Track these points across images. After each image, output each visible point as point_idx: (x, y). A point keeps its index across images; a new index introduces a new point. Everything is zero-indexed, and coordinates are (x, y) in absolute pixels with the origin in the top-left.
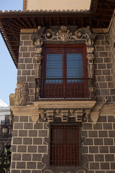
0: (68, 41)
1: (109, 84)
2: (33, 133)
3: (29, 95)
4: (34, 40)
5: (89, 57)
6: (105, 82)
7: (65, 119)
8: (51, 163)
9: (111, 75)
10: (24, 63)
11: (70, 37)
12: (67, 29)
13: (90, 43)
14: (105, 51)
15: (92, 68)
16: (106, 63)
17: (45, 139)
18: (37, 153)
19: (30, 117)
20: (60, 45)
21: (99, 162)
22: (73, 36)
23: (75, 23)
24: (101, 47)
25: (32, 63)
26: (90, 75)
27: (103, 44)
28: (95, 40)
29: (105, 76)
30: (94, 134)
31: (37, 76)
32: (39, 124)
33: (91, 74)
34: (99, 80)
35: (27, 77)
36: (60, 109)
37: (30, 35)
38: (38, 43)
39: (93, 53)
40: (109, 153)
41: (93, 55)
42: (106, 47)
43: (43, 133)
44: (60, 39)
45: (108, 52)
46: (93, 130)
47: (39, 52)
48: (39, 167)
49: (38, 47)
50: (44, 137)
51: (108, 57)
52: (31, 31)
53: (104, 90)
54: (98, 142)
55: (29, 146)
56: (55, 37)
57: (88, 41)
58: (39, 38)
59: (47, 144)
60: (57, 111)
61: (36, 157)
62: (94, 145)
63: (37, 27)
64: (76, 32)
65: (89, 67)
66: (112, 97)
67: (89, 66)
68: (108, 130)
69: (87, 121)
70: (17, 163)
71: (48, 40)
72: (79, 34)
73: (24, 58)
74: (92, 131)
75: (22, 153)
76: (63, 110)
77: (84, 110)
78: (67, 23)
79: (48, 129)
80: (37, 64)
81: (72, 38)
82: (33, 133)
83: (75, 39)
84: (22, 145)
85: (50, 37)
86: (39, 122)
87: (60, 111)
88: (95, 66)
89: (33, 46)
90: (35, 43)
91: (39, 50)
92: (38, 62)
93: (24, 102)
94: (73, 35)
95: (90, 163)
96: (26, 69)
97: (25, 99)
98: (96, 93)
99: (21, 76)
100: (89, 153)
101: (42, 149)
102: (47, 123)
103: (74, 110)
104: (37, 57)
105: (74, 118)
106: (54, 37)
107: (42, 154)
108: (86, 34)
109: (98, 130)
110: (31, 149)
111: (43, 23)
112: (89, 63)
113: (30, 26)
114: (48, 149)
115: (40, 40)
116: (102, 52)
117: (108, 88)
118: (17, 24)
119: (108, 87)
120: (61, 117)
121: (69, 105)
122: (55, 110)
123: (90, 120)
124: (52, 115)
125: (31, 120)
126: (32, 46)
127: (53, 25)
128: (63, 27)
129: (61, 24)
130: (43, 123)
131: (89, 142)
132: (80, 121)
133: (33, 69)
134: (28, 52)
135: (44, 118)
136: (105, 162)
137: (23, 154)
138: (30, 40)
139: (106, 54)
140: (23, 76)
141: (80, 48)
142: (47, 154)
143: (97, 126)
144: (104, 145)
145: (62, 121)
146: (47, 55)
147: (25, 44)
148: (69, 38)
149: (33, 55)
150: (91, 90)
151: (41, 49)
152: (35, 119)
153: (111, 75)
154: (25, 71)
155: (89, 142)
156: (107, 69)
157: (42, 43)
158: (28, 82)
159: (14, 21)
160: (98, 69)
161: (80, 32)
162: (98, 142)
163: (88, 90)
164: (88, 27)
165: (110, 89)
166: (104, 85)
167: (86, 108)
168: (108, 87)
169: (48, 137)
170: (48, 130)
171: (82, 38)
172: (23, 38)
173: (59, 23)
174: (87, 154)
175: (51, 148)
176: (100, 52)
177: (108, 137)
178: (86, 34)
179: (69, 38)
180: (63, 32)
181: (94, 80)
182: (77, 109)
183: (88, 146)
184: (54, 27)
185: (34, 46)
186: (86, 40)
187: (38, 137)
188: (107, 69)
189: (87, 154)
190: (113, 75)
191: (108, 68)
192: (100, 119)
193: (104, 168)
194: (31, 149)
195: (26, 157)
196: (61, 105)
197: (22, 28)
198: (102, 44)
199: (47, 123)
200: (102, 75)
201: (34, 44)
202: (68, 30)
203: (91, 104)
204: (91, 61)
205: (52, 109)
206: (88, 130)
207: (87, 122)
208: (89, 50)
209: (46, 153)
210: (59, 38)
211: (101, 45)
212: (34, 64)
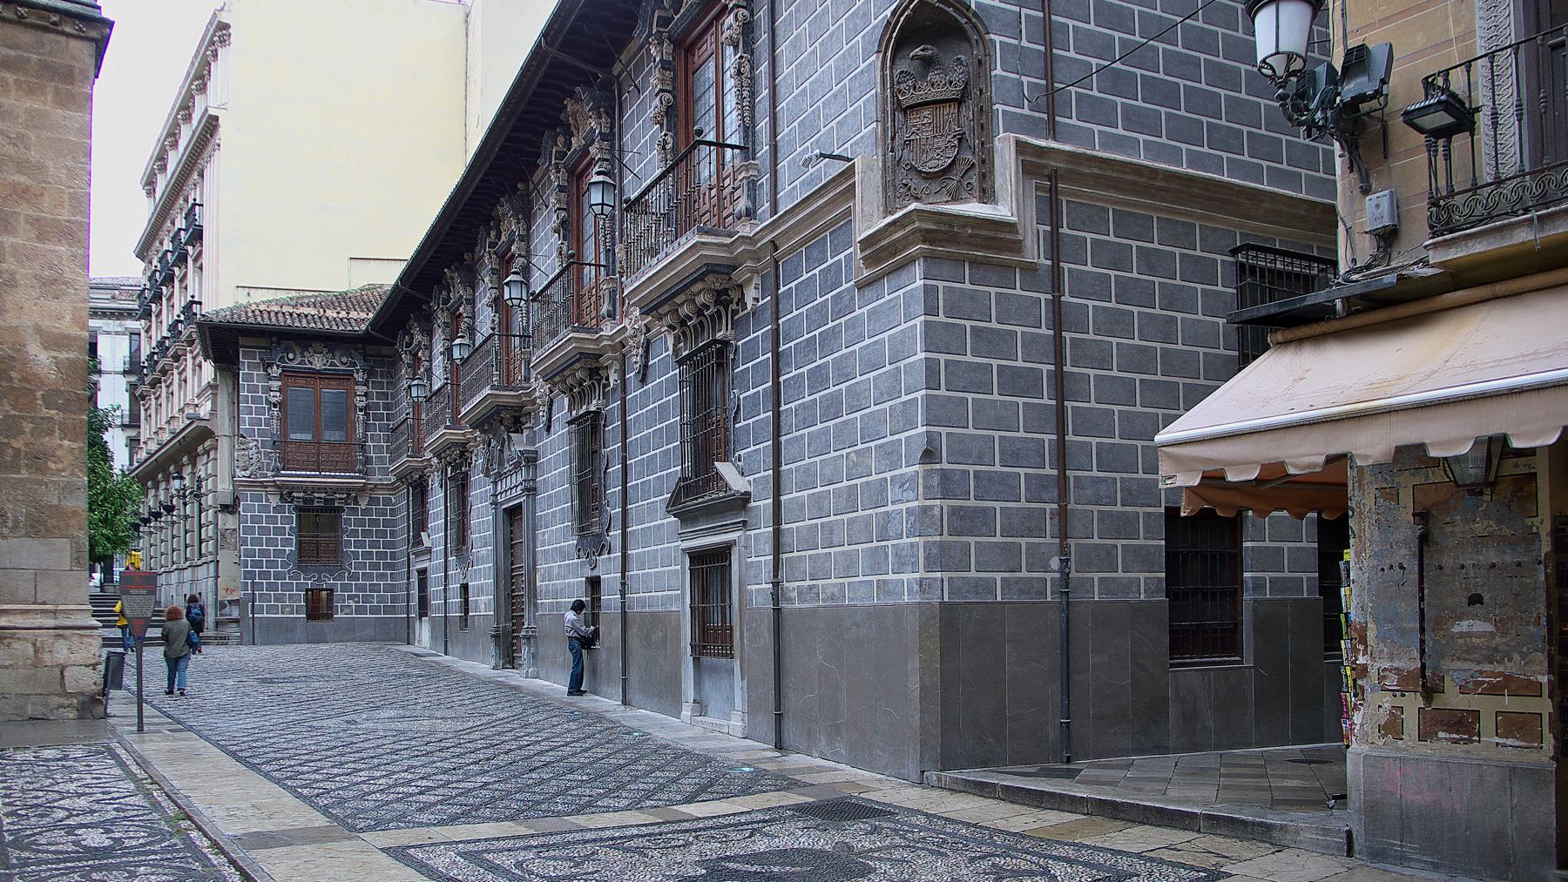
2: (272, 520)
4: (267, 366)
13: (359, 377)
38: (275, 371)
39: (366, 395)
43: (288, 520)
91: (276, 384)
101: (286, 542)
143: (366, 512)
162: (366, 533)
175: (300, 544)
194: (270, 542)
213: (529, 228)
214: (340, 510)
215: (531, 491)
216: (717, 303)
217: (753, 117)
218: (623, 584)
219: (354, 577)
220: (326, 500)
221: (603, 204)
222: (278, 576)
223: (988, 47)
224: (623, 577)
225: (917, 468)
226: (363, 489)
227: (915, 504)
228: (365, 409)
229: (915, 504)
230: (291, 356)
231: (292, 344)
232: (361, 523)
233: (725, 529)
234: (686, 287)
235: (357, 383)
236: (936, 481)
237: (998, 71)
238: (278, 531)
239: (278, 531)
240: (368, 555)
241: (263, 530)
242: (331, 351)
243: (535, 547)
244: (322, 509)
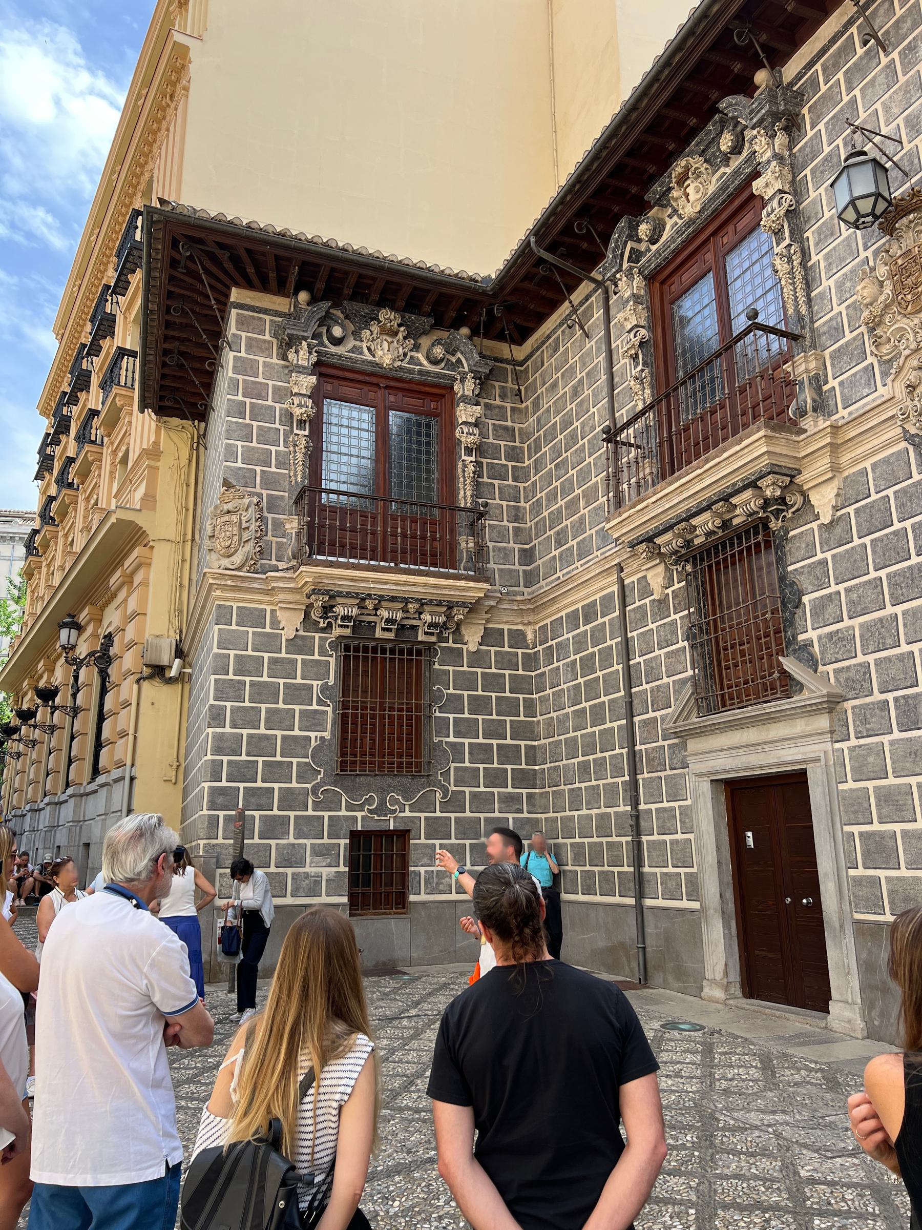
0: (400, 367)
1: (517, 531)
2: (282, 667)
3: (269, 537)
4: (288, 343)
5: (466, 437)
6: (505, 523)
7: (390, 630)
8: (343, 765)
9: (522, 504)
10: (247, 421)
11: (405, 355)
12: (400, 325)
13: (468, 387)
14: (509, 423)
15: (472, 475)
16: (510, 464)
17: (324, 689)
18: (297, 732)
19: (273, 611)
20: (372, 374)
21: (481, 766)
22: (415, 354)
23: (427, 309)
24: (499, 407)
25: (277, 425)
26: (465, 497)
28: (484, 381)
29: (504, 503)
30: (468, 682)
31: (299, 476)
32: (303, 637)
33: (469, 493)
35: (258, 472)
36: (381, 598)
37: (268, 318)
38: (303, 356)
40: (509, 741)
41: (476, 431)
42: (513, 409)
43: (316, 669)
44: (374, 356)
45: (517, 426)
46: (465, 668)
47: (304, 392)
48: (301, 778)
49: (300, 369)
50: (320, 683)
51: (517, 444)
52: (281, 303)
53: (500, 549)
54: (479, 705)
55: (268, 711)
56: (358, 343)
57: (463, 381)
58: (305, 338)
59: (329, 706)
60: (370, 604)
61: (293, 745)
62: (466, 715)
63: (296, 293)
64: (425, 342)
65: (464, 471)
66: (521, 574)
67: (465, 466)
68: (507, 672)
69: (451, 641)
70: (230, 763)
71: (333, 349)
72: (438, 351)
73: (248, 401)
74: (464, 672)
75: (245, 732)
76: (387, 600)
78: (401, 304)
79: (331, 656)
80: (296, 431)
82: (282, 667)
83: (421, 364)
84: (247, 704)
85: (338, 342)
86: (301, 633)
87: (380, 601)
89: (278, 362)
90: (291, 356)
92: (301, 423)
93: (252, 559)
94: (416, 347)
95: (456, 768)
96: (254, 444)
97: (258, 549)
98: (481, 551)
99: (239, 465)
100: (452, 739)
101: (312, 720)
102: (327, 638)
103: (422, 603)
104: (298, 406)
105: (414, 628)
106: (351, 343)
107: (312, 735)
108: (459, 355)
109: (479, 670)
110: (277, 719)
111: (320, 285)
112: (464, 457)
113: (255, 279)
114: (334, 720)
115: (309, 345)
116: (500, 426)
117: (511, 545)
118: (228, 265)
119: (511, 541)
120: (376, 623)
121: (410, 589)
122: (363, 600)
123: (459, 639)
124: (355, 611)
125: (275, 623)
126: (274, 360)
127: (354, 297)
128: (385, 315)
129: (382, 303)
130: (317, 635)
131: (455, 704)
132: (433, 639)
133: (282, 448)
134: (260, 379)
135: (321, 621)
136: (496, 765)
137: (250, 736)
138: (267, 337)
139: (510, 432)
140: (245, 466)
142: (327, 735)
143: (478, 659)
144: (494, 717)
145: (379, 633)
146: (325, 402)
147: (249, 348)
148: (402, 358)
149: (281, 394)
150: (466, 544)
151: (313, 379)
152: (290, 624)
153: (522, 504)
154: (253, 448)
155: (455, 704)
156: (510, 482)
157: (314, 358)
158: (265, 492)
159: (224, 256)
160: (485, 479)
161: (439, 343)
162: (479, 705)
164: (465, 331)
165: (516, 546)
167: (458, 602)
168: (511, 541)
169: (331, 682)
170: (332, 661)
171: (443, 365)
172: (243, 324)
173: (375, 297)
174: (447, 739)
175: (344, 721)
176: (494, 425)
177: (508, 694)
178: (459, 355)
179: (402, 358)
180: (384, 331)
181: (479, 514)
182: (430, 603)
183: (451, 716)
184: (356, 306)
185: (283, 362)
186: (458, 377)
187: (299, 680)
188: (510, 482)
189: (447, 739)
190: (527, 506)
191: (515, 480)
192: (490, 637)
193: (493, 783)
194: (277, 719)
195: (259, 745)
196: (388, 587)
197: (237, 285)
198: (500, 396)
199: (327, 638)
200: (498, 501)
201: (285, 358)
202: (402, 329)
203: (474, 590)
204: (469, 451)
205: (357, 594)
206: (451, 669)
207: (451, 644)
208: (465, 413)
209: (324, 734)
210: (369, 349)
211: (498, 402)
212: (282, 428)
219: (454, 802)
222: (290, 800)
226: (473, 608)
228: (479, 450)
232: (468, 682)
235: (465, 399)
238: (298, 694)
239: (298, 694)
240: (482, 753)
241: (263, 692)
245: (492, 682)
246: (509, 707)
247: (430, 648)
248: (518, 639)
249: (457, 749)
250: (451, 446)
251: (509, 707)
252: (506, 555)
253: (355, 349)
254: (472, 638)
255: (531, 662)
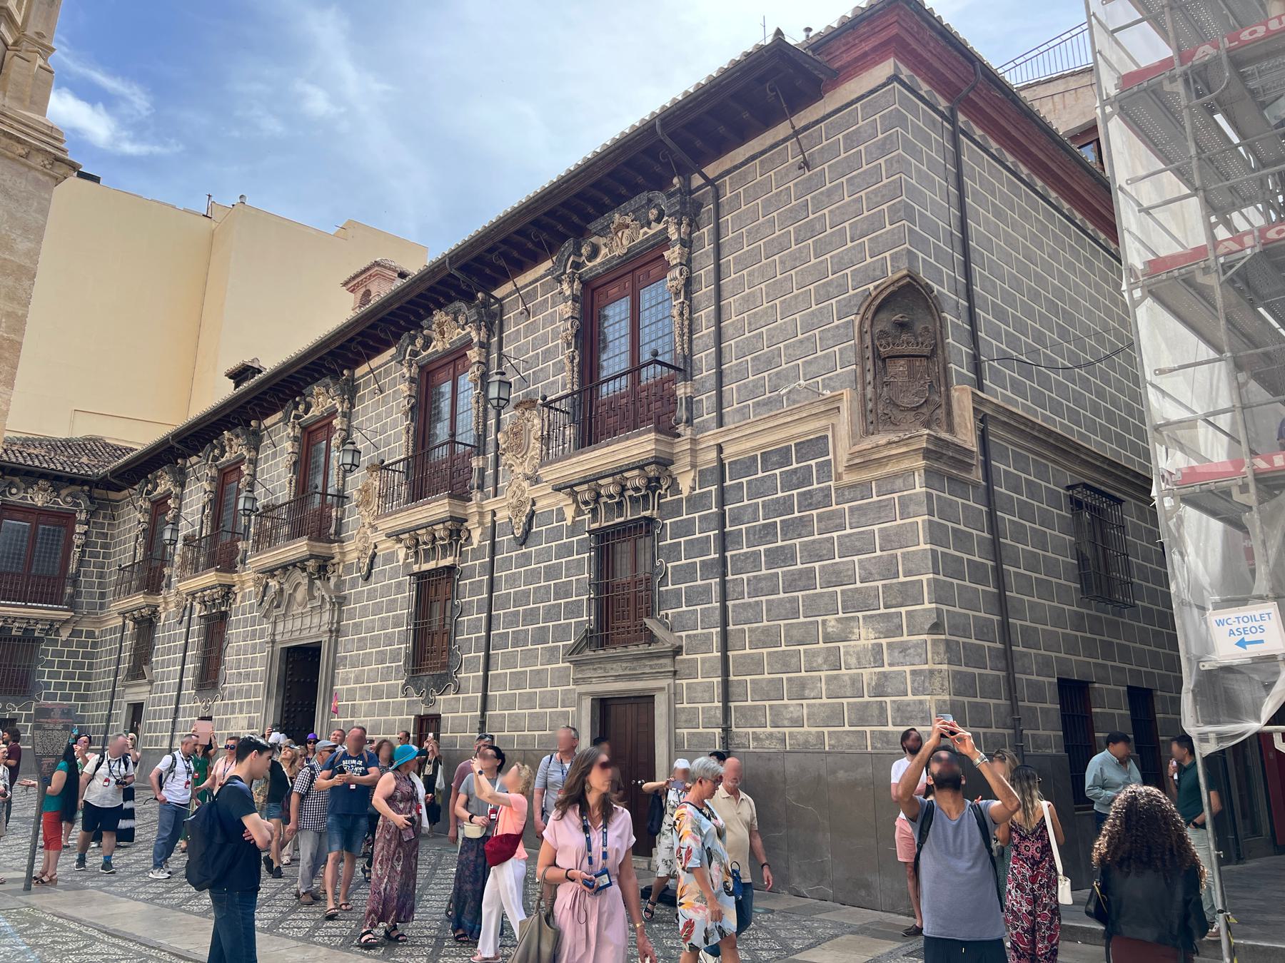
5: (78, 540)
27: (104, 518)
30: (59, 654)
34: (85, 575)
39: (85, 533)
64: (64, 492)
77: (53, 621)
81: (55, 502)
88: (83, 552)
94: (58, 496)
98: (77, 594)
103: (37, 621)
139: (105, 535)
141: (67, 519)
143: (65, 644)
150: (69, 590)
162: (63, 665)
163: (63, 589)
166: (91, 585)
180: (40, 489)
203: (67, 615)
208: (79, 529)
213: (353, 406)
214: (40, 640)
215: (336, 632)
216: (647, 488)
217: (690, 349)
218: (483, 723)
220: (26, 629)
221: (499, 398)
223: (943, 321)
224: (483, 715)
225: (924, 637)
226: (67, 621)
227: (926, 667)
229: (926, 667)
230: (14, 491)
231: (17, 480)
232: (59, 654)
233: (655, 675)
234: (622, 472)
235: (81, 523)
236: (942, 648)
237: (950, 340)
240: (61, 686)
242: (57, 490)
243: (333, 684)
244: (19, 639)
245: (73, 654)
246: (80, 666)
247: (40, 640)
248: (90, 634)
249: (48, 685)
250: (70, 544)
251: (80, 666)
252: (91, 595)
253: (24, 498)
254: (65, 634)
255: (94, 645)
